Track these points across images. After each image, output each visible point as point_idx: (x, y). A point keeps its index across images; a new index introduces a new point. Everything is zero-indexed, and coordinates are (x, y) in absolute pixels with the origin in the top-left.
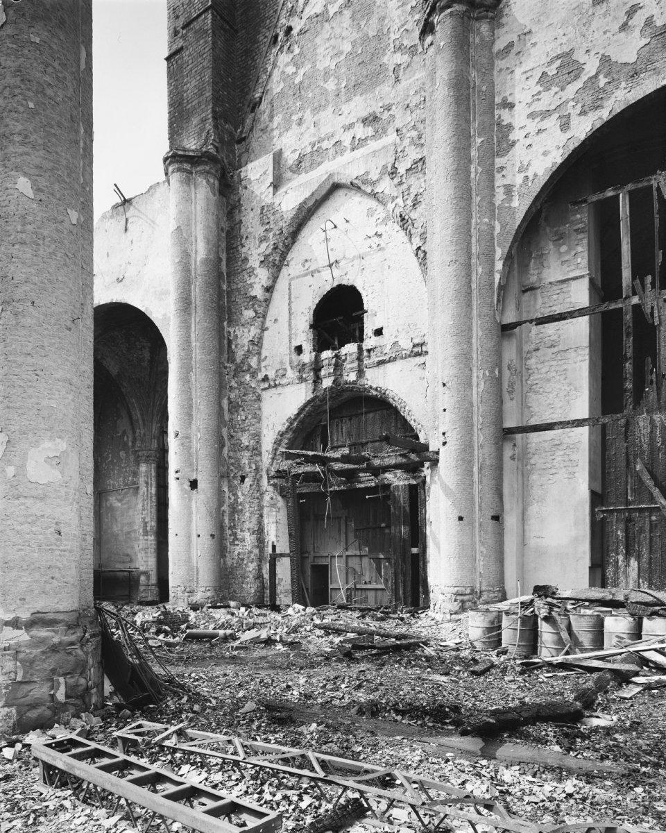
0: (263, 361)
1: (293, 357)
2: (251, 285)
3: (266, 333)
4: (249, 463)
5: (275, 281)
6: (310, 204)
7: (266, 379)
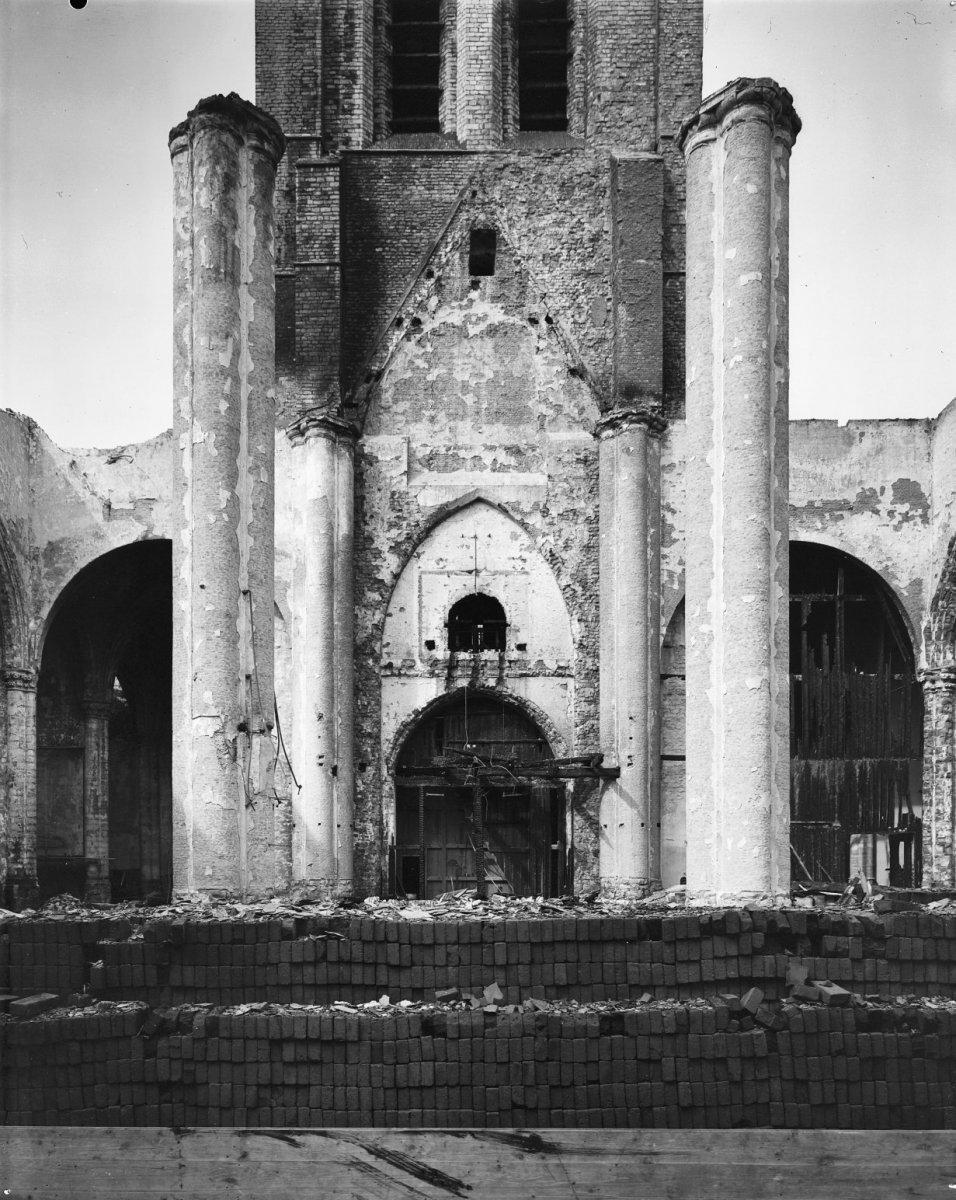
0: (384, 646)
1: (424, 650)
2: (377, 568)
3: (388, 619)
4: (373, 751)
5: (402, 570)
6: (452, 508)
7: (390, 666)
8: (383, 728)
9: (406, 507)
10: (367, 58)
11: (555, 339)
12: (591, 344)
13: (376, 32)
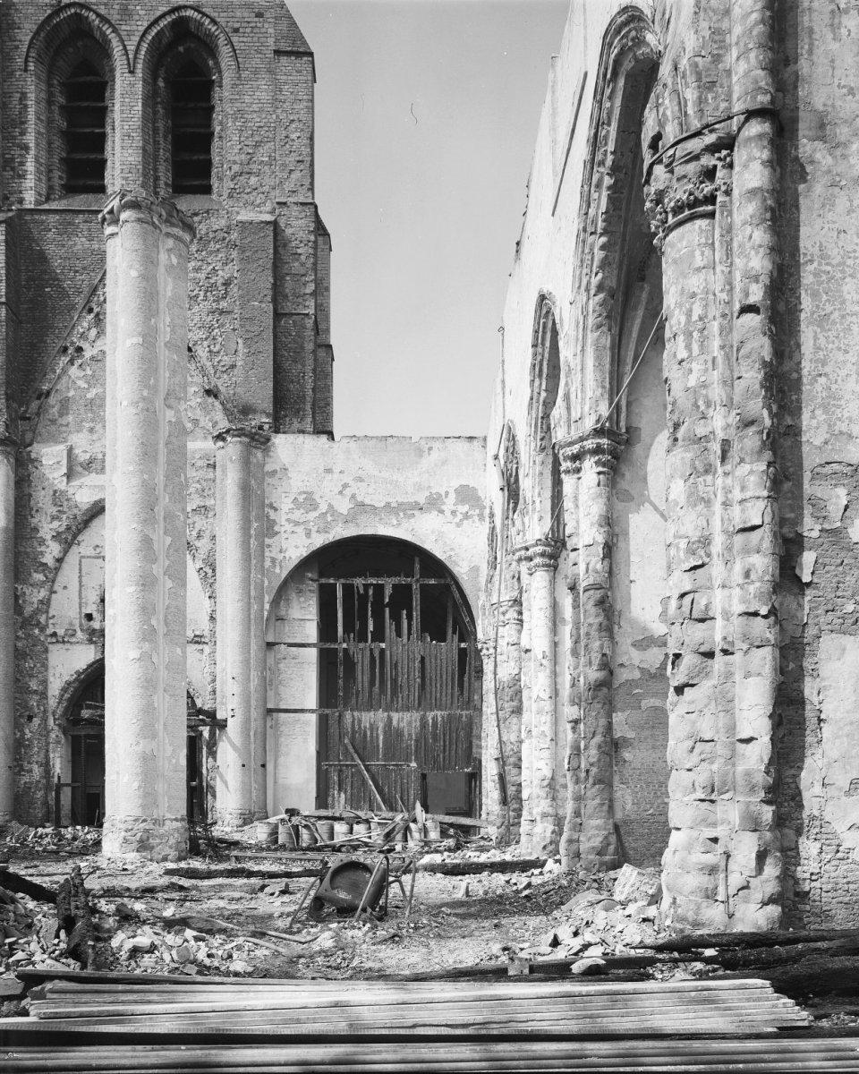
0: (50, 619)
3: (53, 595)
4: (38, 705)
5: (65, 555)
7: (55, 634)
8: (50, 686)
9: (66, 503)
10: (38, 133)
11: (194, 365)
12: (224, 369)
13: (50, 111)
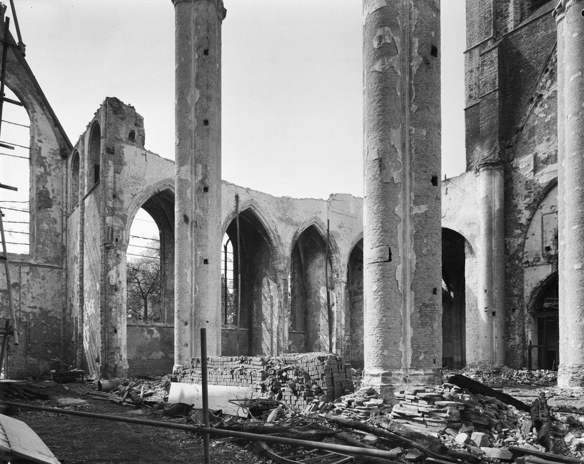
0: (525, 253)
2: (520, 218)
3: (527, 240)
4: (518, 303)
5: (533, 216)
7: (527, 262)
8: (525, 291)
9: (533, 186)
